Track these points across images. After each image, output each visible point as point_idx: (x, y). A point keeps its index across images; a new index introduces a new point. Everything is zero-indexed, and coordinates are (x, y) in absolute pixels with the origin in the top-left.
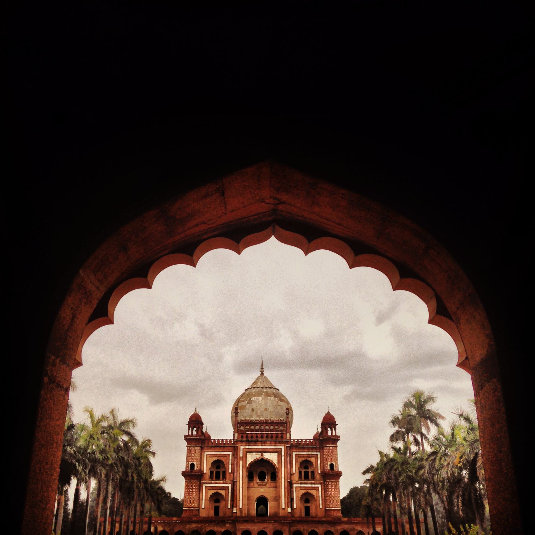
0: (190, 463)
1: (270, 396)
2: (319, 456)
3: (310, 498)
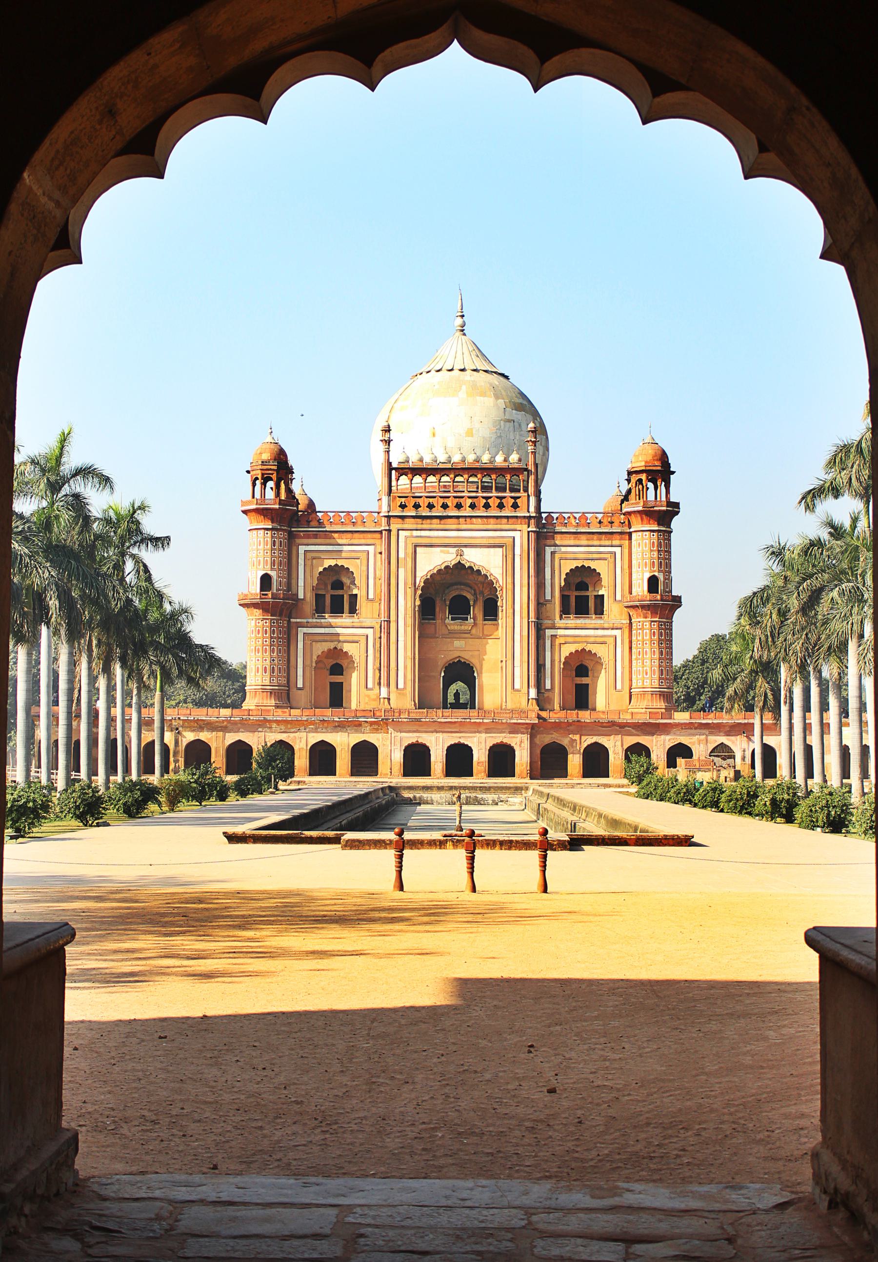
1: (483, 394)
3: (587, 663)
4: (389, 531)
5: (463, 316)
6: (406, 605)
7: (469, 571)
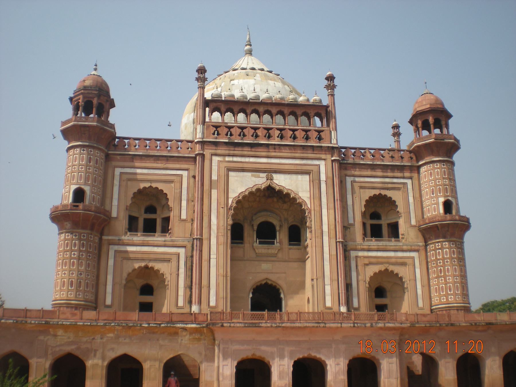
0: (74, 187)
2: (410, 186)
3: (387, 286)
4: (203, 156)
5: (251, 45)
6: (217, 225)
7: (275, 200)
